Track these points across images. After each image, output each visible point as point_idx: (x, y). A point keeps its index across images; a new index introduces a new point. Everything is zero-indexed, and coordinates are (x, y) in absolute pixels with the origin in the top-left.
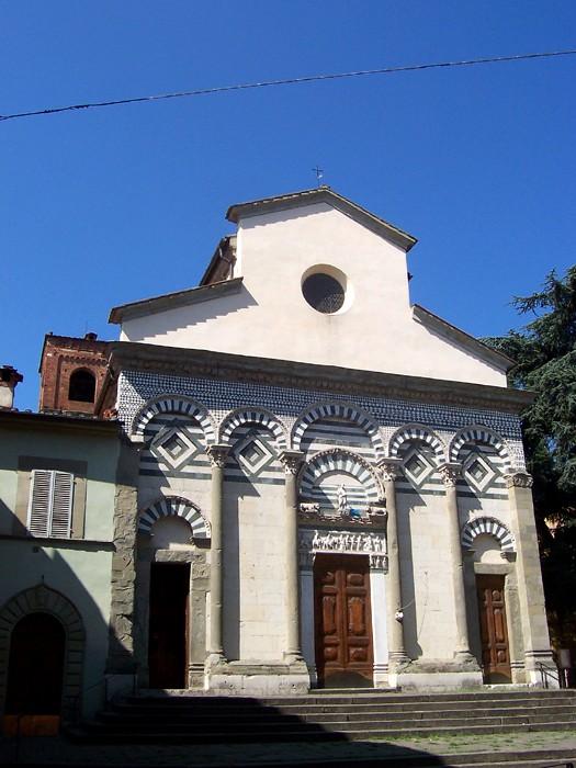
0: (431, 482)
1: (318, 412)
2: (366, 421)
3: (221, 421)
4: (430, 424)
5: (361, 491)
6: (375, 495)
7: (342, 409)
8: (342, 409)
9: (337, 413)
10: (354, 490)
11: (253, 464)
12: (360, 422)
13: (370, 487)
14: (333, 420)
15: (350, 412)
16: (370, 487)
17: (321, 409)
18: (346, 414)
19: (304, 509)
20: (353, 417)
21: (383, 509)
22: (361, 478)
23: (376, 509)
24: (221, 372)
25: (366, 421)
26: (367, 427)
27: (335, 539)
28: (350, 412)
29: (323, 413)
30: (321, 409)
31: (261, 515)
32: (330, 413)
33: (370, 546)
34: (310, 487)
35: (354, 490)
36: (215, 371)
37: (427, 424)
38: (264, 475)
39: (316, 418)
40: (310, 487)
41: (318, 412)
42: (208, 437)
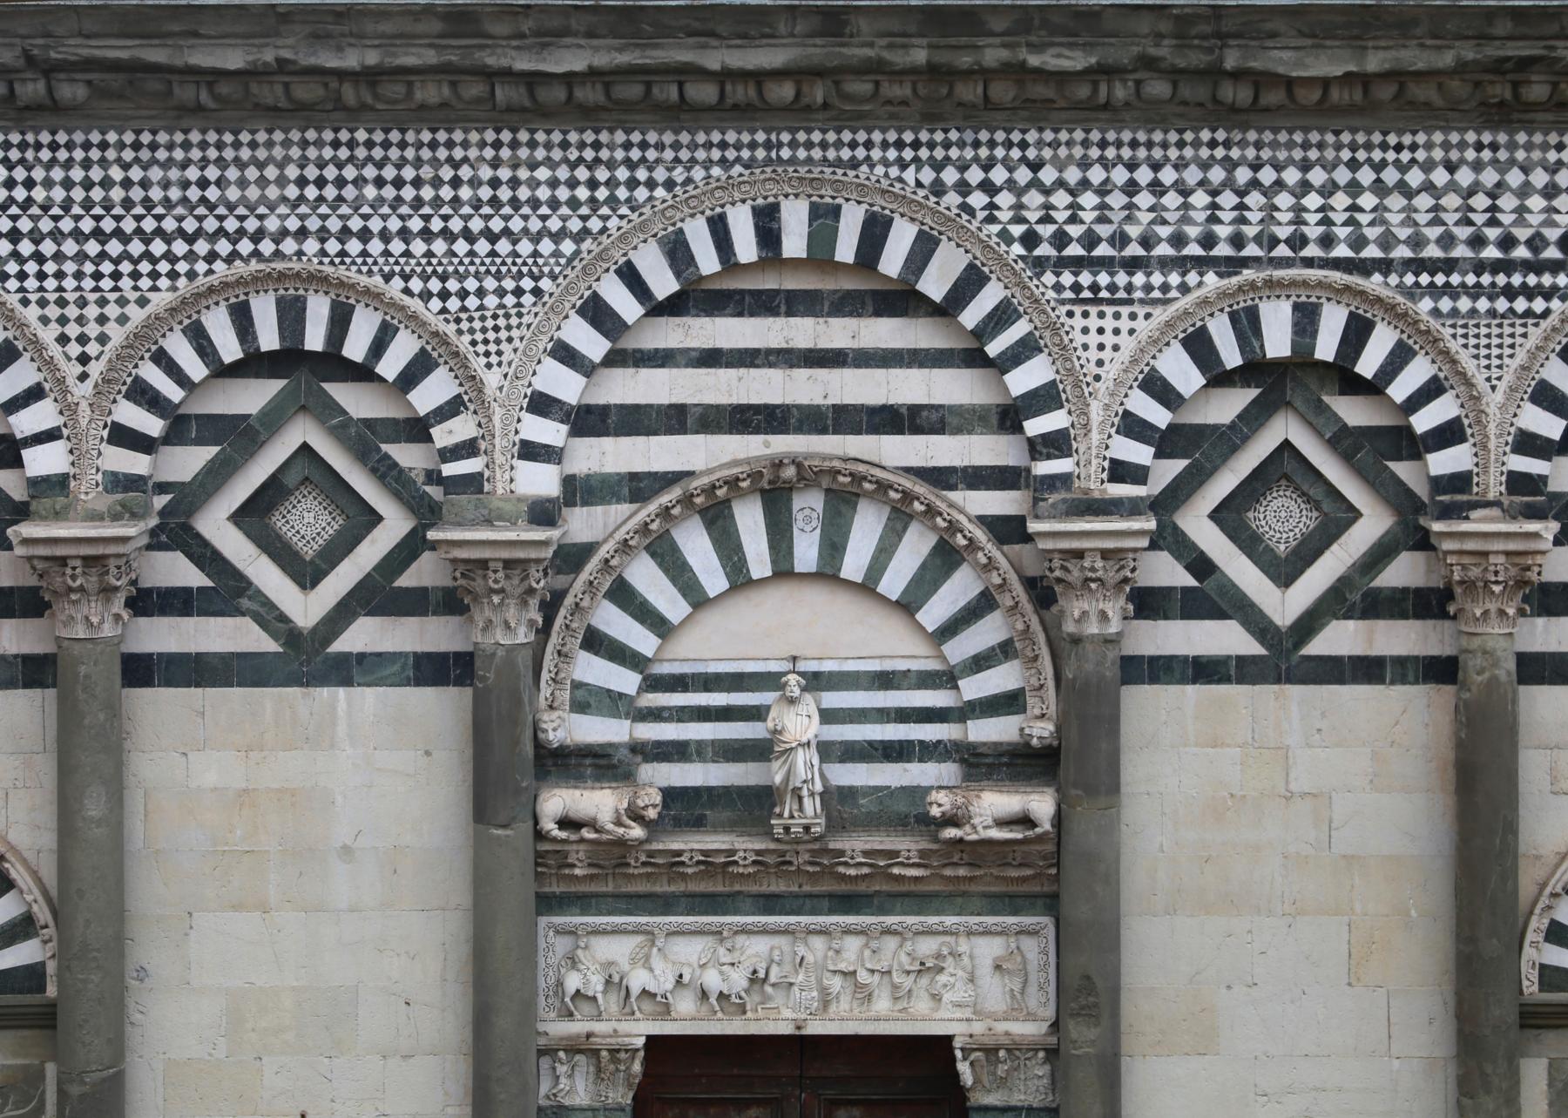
0: (1379, 606)
1: (678, 252)
2: (969, 283)
3: (95, 369)
4: (1385, 266)
5: (947, 679)
6: (1009, 703)
7: (824, 218)
8: (824, 218)
9: (794, 244)
10: (885, 680)
11: (307, 574)
12: (934, 285)
13: (980, 663)
14: (768, 282)
15: (875, 233)
16: (980, 663)
17: (699, 237)
18: (846, 250)
19: (565, 823)
20: (892, 262)
21: (1042, 805)
22: (935, 613)
23: (994, 804)
24: (71, 91)
25: (969, 283)
26: (971, 317)
27: (756, 949)
28: (875, 233)
29: (707, 261)
30: (699, 237)
31: (347, 851)
32: (746, 248)
33: (962, 985)
34: (625, 681)
35: (885, 680)
36: (32, 89)
37: (1364, 268)
38: (362, 636)
39: (664, 284)
40: (625, 681)
41: (678, 252)
42: (43, 461)
